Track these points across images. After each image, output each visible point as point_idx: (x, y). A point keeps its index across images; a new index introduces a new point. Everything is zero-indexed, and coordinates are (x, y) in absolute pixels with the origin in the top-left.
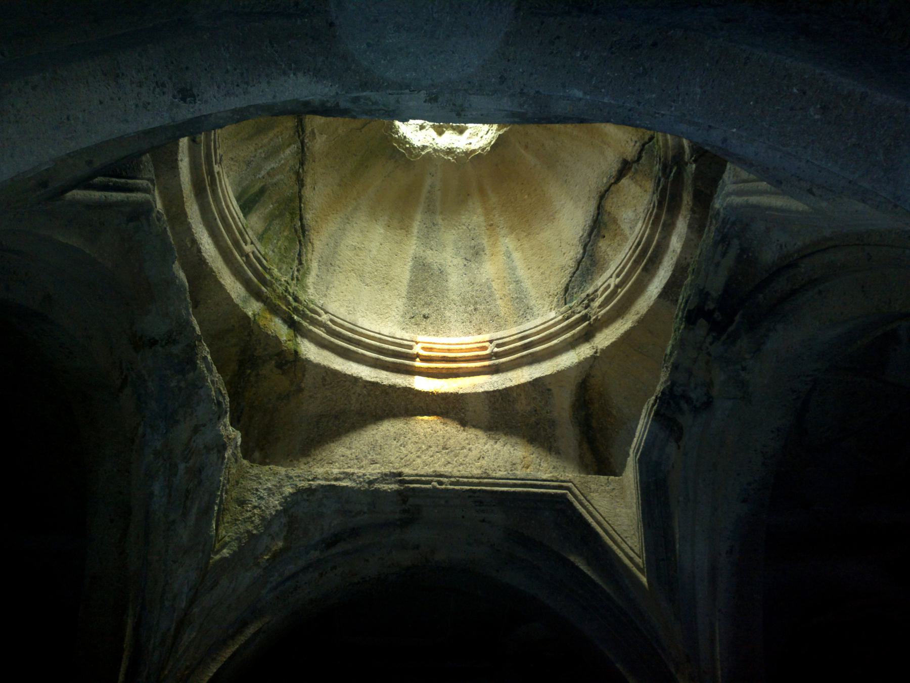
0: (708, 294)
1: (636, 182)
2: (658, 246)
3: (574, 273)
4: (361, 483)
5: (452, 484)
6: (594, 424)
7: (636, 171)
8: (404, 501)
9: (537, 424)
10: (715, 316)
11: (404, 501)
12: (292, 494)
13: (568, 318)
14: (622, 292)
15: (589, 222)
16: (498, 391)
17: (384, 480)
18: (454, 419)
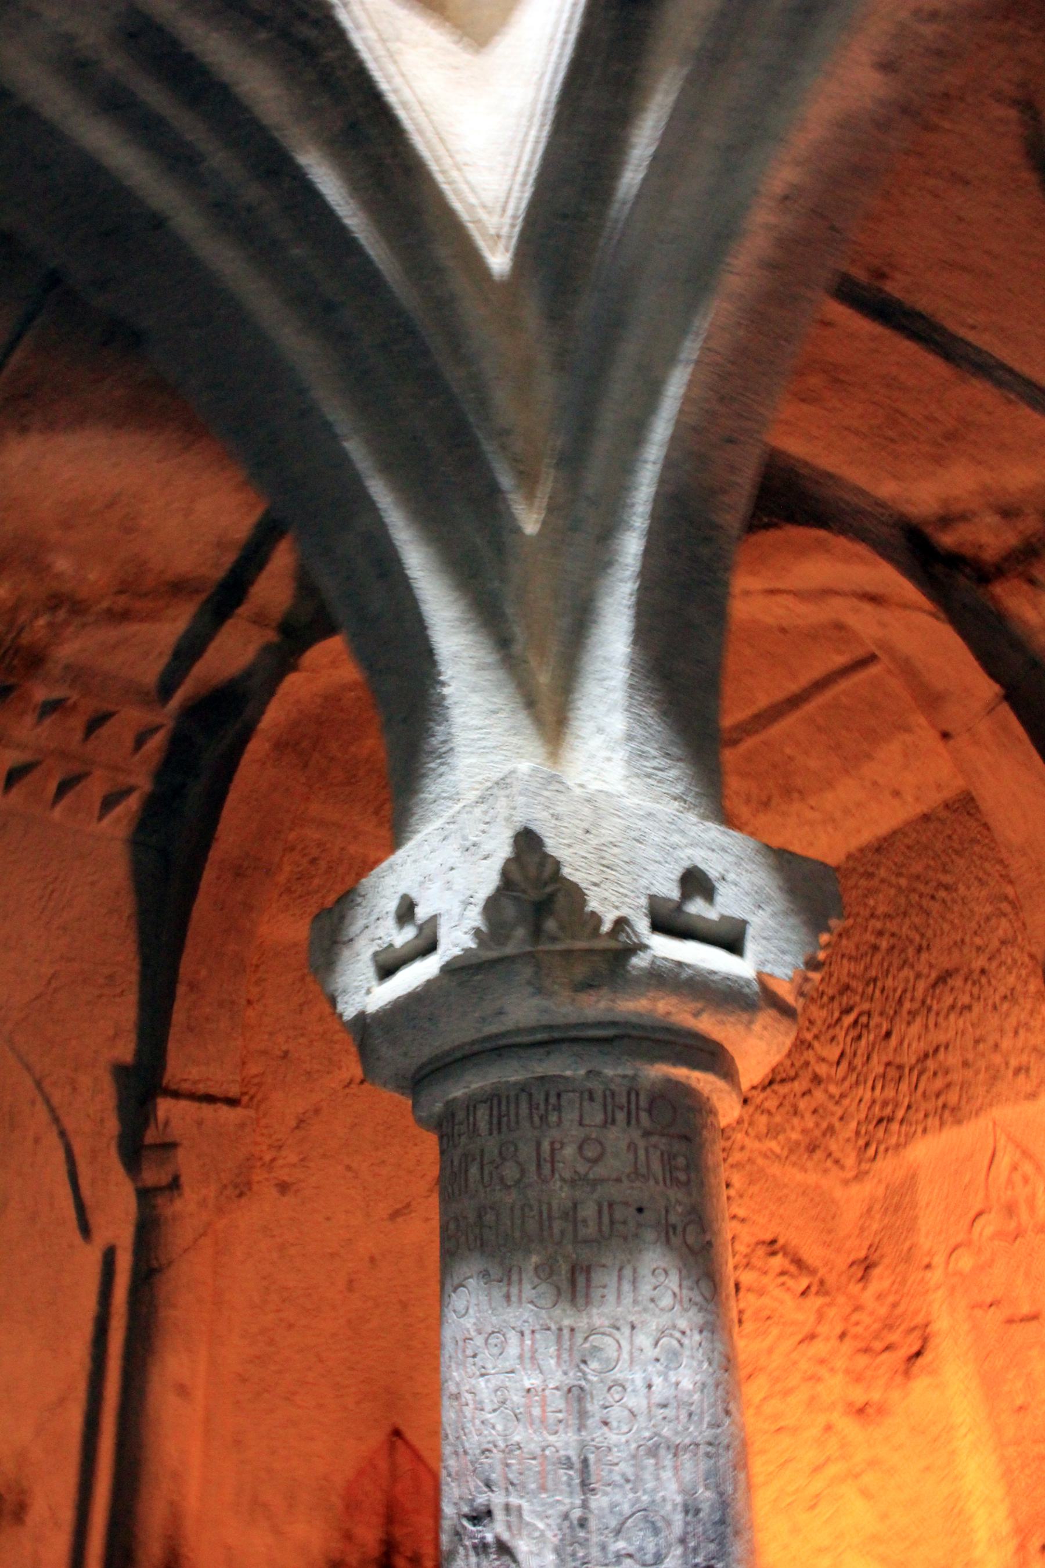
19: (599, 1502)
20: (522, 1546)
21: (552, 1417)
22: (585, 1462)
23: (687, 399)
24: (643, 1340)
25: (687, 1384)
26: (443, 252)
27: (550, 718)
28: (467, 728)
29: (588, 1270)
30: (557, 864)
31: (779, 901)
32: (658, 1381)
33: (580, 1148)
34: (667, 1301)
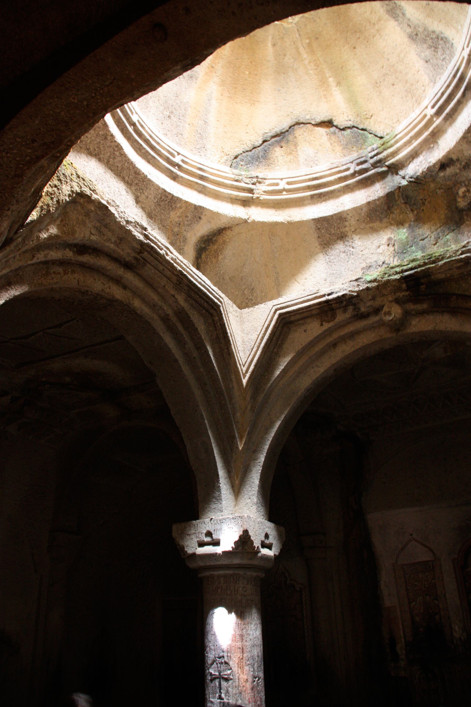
0: (430, 276)
1: (330, 139)
2: (332, 192)
3: (247, 151)
4: (121, 218)
5: (172, 259)
6: (203, 256)
7: (334, 133)
8: (140, 252)
9: (178, 235)
10: (422, 287)
11: (140, 252)
12: (77, 194)
13: (237, 181)
14: (285, 196)
15: (278, 130)
16: (173, 196)
17: (136, 227)
18: (133, 193)
19: (245, 655)
20: (231, 663)
21: (237, 640)
22: (243, 648)
23: (279, 428)
24: (252, 626)
25: (258, 634)
26: (233, 377)
27: (237, 491)
28: (223, 494)
29: (244, 613)
30: (250, 537)
31: (277, 539)
32: (254, 633)
33: (243, 588)
34: (255, 619)
